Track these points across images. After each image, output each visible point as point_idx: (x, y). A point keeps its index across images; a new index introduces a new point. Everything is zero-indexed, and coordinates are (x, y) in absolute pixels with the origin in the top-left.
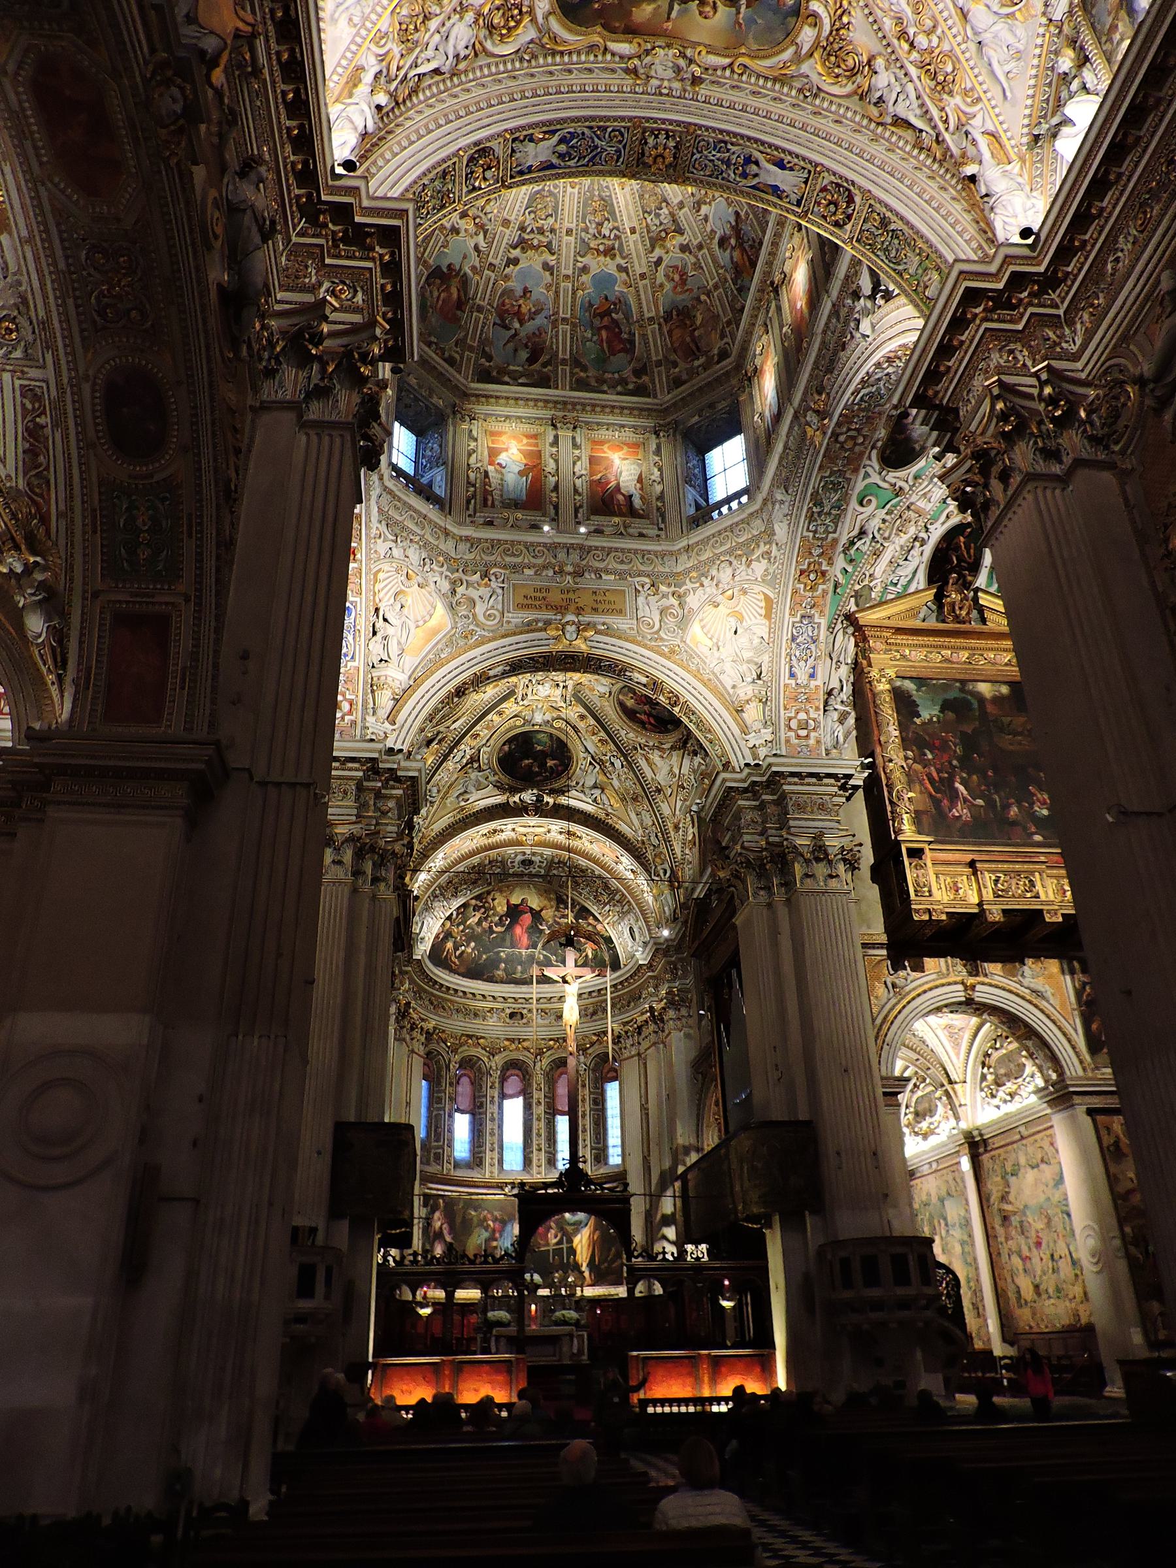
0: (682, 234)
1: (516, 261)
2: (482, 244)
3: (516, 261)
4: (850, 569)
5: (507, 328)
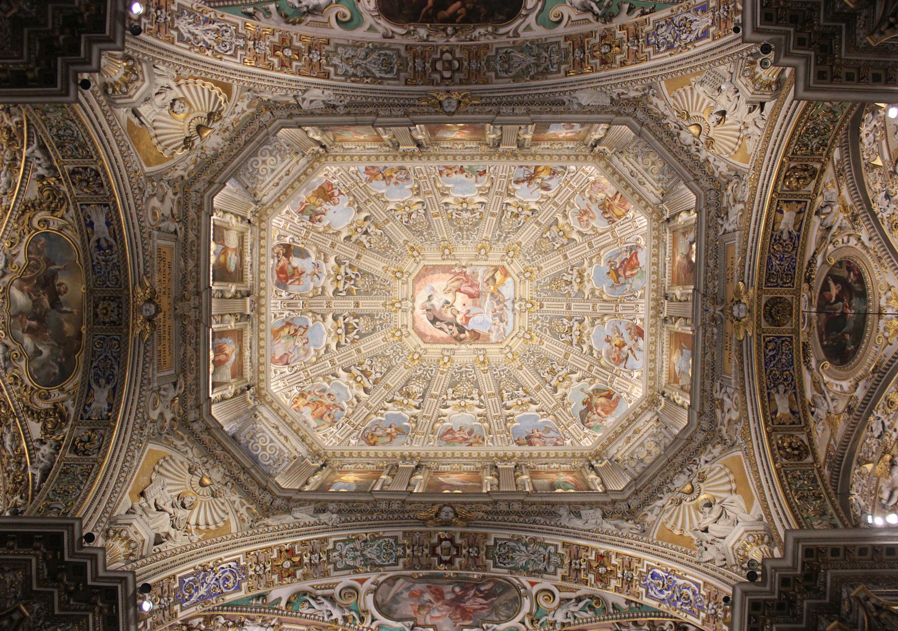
0: (557, 220)
1: (591, 348)
2: (579, 374)
3: (591, 348)
4: (626, 6)
5: (627, 358)
